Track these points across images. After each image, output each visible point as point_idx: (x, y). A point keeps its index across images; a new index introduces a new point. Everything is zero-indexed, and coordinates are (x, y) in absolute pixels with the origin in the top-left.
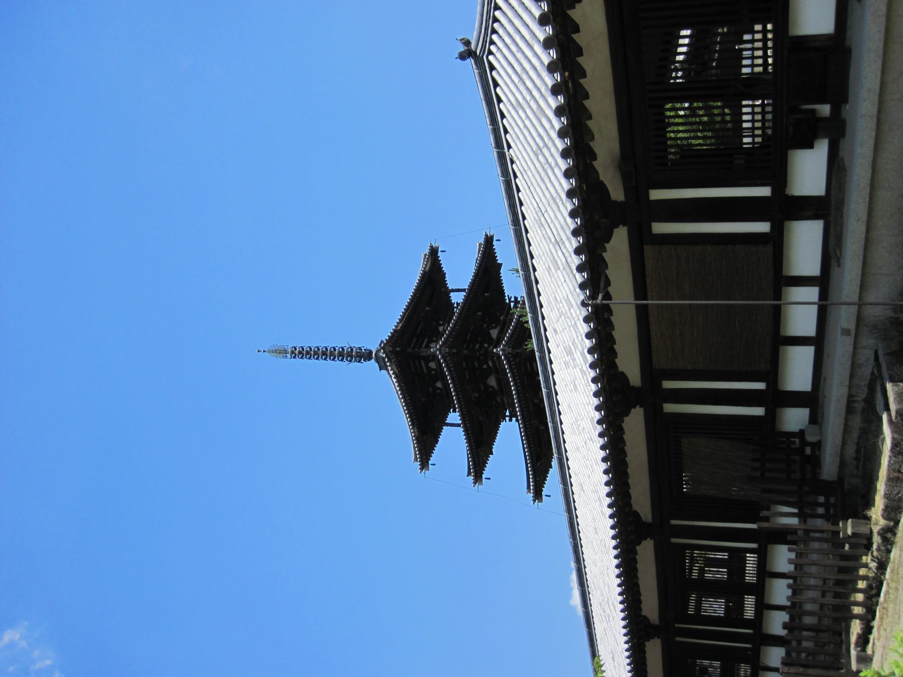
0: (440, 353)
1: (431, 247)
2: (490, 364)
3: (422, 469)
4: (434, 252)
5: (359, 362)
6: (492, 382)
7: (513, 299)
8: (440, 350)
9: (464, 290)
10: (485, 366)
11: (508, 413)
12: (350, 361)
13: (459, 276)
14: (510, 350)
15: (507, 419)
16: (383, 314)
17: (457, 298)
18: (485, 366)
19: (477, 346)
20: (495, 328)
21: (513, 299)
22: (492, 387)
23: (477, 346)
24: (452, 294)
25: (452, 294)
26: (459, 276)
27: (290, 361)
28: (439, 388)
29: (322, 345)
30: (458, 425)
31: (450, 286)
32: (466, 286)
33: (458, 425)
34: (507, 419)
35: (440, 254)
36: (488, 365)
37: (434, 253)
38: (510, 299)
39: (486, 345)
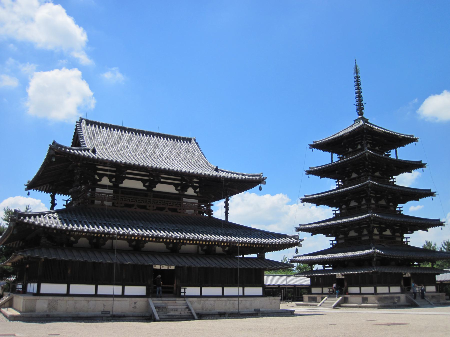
0: (365, 152)
1: (417, 139)
2: (362, 174)
3: (310, 145)
4: (414, 140)
5: (357, 110)
6: (354, 175)
7: (394, 180)
8: (367, 152)
9: (397, 157)
10: (361, 171)
11: (340, 183)
12: (356, 105)
13: (403, 154)
14: (369, 186)
15: (337, 183)
16: (382, 120)
17: (392, 154)
18: (361, 171)
19: (370, 167)
20: (380, 174)
21: (394, 180)
22: (351, 175)
23: (370, 167)
24: (394, 150)
25: (394, 150)
26: (403, 154)
27: (353, 75)
28: (348, 150)
29: (363, 94)
30: (332, 161)
31: (397, 149)
32: (398, 158)
33: (332, 161)
34: (337, 183)
35: (414, 143)
36: (362, 173)
37: (414, 140)
38: (395, 179)
39: (371, 171)
